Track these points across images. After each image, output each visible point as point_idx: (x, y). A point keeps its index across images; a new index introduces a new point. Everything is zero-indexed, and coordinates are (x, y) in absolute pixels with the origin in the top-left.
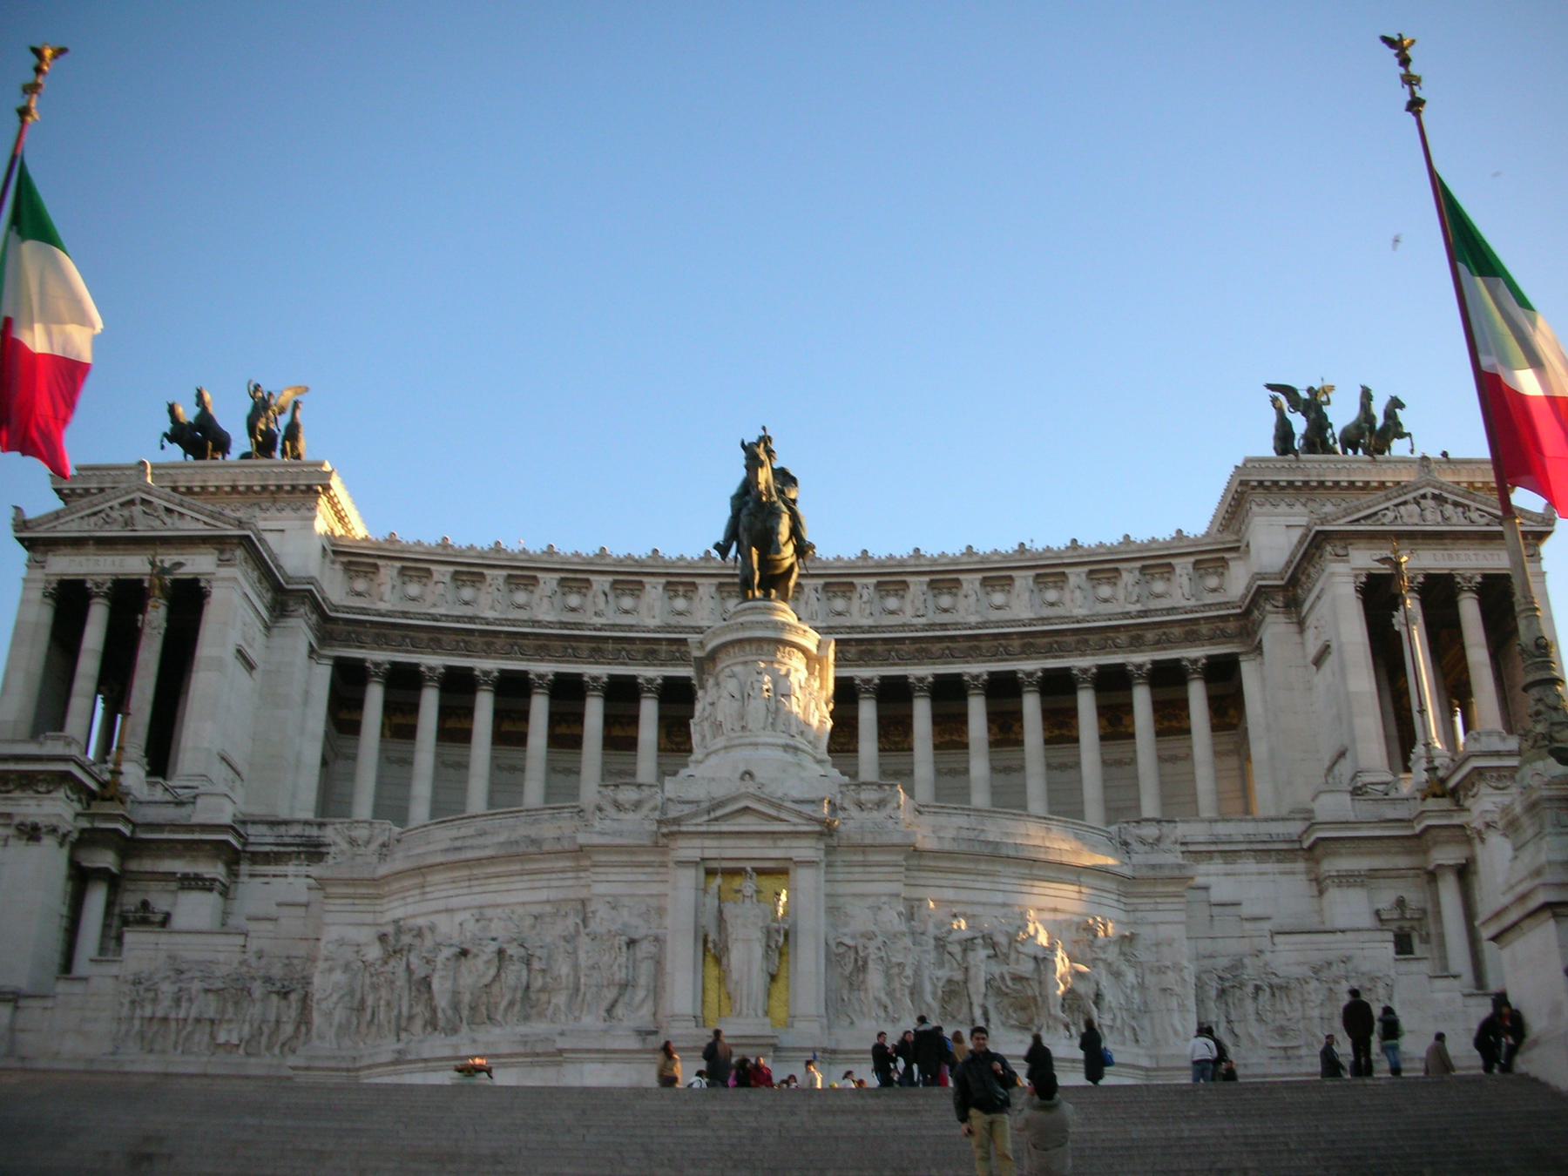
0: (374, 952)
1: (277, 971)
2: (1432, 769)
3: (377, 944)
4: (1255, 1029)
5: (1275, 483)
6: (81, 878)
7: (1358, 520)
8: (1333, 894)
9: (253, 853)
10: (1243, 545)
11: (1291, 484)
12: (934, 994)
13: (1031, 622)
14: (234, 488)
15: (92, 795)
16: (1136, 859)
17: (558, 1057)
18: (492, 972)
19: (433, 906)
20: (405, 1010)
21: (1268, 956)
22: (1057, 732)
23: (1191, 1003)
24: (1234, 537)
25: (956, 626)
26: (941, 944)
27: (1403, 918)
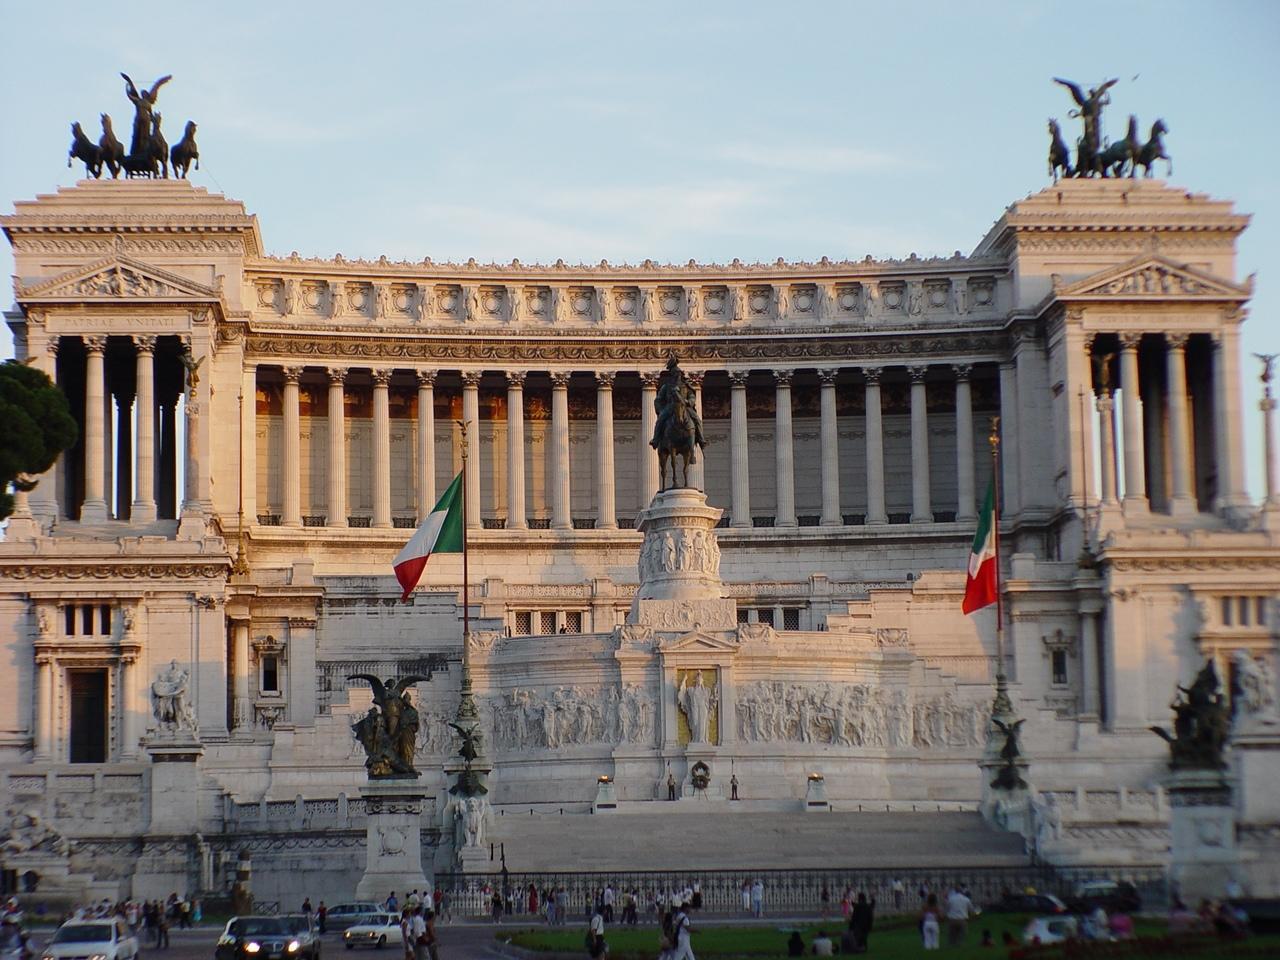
0: (500, 703)
1: (438, 708)
2: (1087, 549)
3: (503, 699)
4: (944, 735)
5: (1038, 228)
6: (232, 625)
7: (1092, 290)
8: (1018, 626)
9: (330, 600)
10: (1011, 268)
11: (1051, 229)
12: (785, 727)
13: (834, 328)
14: (168, 229)
15: (230, 571)
16: (885, 649)
17: (611, 761)
18: (573, 719)
19: (535, 682)
20: (525, 735)
21: (952, 697)
22: (847, 405)
23: (911, 725)
24: (1003, 261)
25: (768, 330)
26: (789, 704)
27: (1060, 642)
